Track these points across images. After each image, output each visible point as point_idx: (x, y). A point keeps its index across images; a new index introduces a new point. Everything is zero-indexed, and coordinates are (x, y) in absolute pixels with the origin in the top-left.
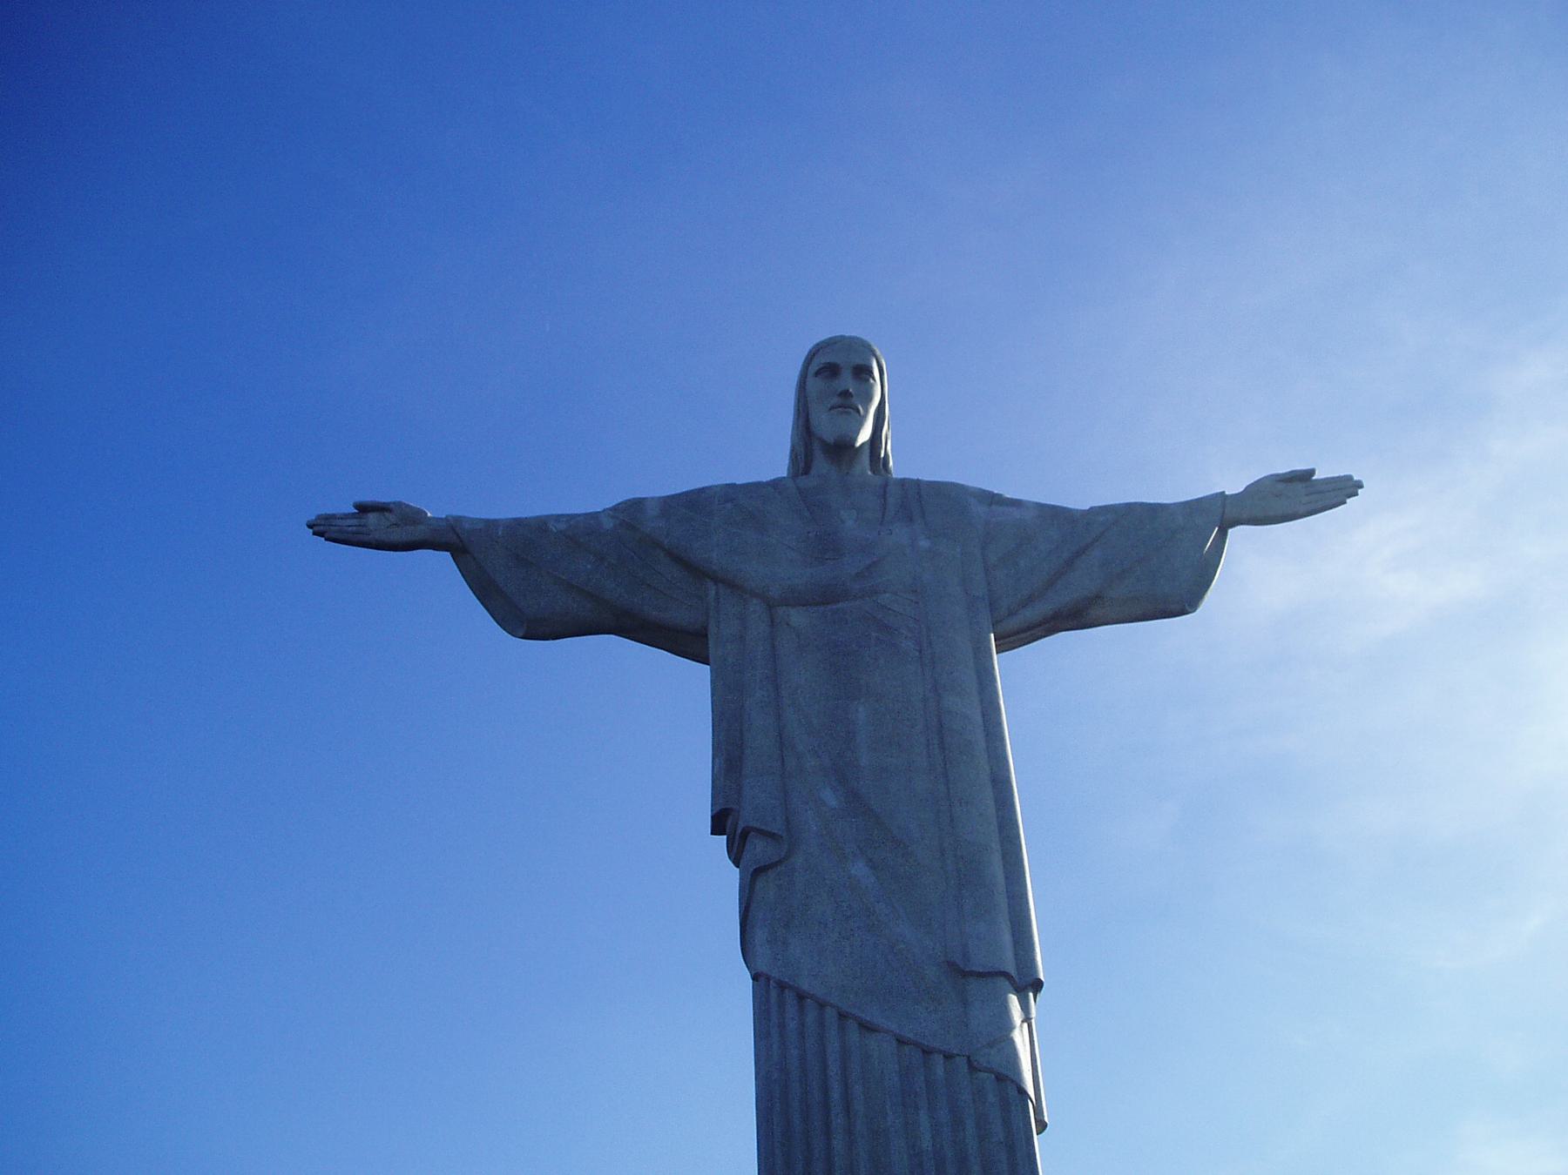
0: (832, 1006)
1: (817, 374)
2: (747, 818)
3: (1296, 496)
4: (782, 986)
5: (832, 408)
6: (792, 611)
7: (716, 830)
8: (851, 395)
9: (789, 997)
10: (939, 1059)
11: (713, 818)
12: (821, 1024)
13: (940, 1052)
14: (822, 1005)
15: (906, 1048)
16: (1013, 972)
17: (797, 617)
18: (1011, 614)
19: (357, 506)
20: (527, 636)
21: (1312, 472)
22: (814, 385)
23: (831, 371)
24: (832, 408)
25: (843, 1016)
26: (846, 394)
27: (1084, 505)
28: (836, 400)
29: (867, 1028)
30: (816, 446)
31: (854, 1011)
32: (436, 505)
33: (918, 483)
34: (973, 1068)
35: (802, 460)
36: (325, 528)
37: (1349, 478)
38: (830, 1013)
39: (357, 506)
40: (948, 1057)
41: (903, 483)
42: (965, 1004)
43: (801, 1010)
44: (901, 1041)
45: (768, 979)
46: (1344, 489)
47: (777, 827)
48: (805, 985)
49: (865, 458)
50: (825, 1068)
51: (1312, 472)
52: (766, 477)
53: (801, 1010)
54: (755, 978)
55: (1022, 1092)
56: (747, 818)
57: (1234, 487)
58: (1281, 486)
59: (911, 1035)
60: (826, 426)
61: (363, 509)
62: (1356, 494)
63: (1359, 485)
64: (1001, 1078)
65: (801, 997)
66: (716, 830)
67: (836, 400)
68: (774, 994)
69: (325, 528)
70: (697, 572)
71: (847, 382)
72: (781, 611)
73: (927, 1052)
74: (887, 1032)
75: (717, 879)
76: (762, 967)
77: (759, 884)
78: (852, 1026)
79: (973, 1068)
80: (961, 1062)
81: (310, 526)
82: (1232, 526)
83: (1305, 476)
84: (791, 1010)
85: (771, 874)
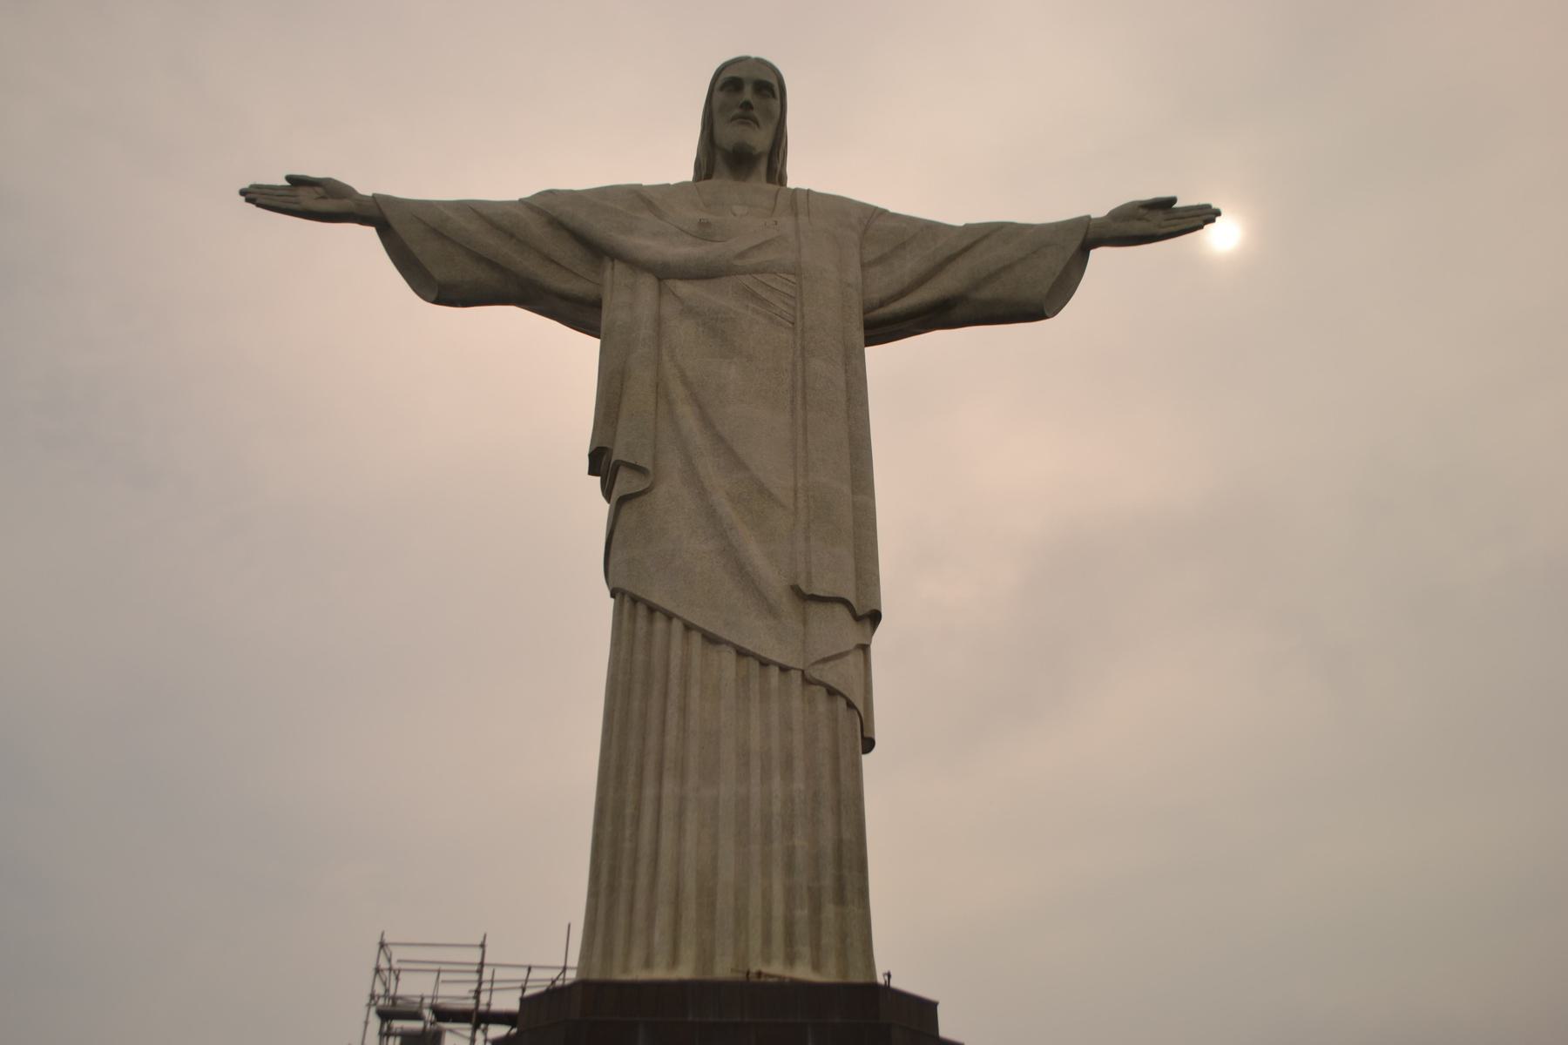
0: (678, 618)
1: (722, 88)
2: (619, 454)
3: (1159, 220)
4: (635, 600)
5: (733, 119)
6: (679, 284)
7: (592, 472)
8: (751, 108)
9: (642, 610)
10: (774, 671)
11: (590, 455)
12: (669, 633)
13: (775, 663)
14: (670, 617)
15: (744, 661)
16: (851, 598)
17: (683, 288)
18: (882, 304)
19: (289, 178)
20: (438, 301)
21: (1174, 200)
22: (719, 97)
24: (733, 119)
25: (688, 627)
26: (747, 106)
27: (959, 221)
28: (737, 111)
29: (711, 639)
30: (719, 157)
31: (701, 624)
32: (365, 185)
33: (809, 191)
34: (807, 681)
35: (705, 168)
36: (257, 196)
37: (1209, 206)
38: (677, 626)
39: (289, 178)
40: (784, 669)
41: (796, 190)
42: (805, 622)
43: (651, 620)
44: (741, 653)
45: (623, 593)
46: (1205, 215)
47: (644, 462)
48: (656, 599)
49: (762, 167)
50: (667, 673)
51: (1174, 200)
52: (673, 179)
53: (651, 620)
54: (613, 595)
55: (850, 705)
56: (619, 454)
57: (1099, 210)
58: (1142, 211)
59: (750, 647)
60: (730, 135)
61: (296, 181)
62: (1213, 221)
63: (1218, 213)
64: (832, 692)
65: (652, 609)
66: (592, 472)
67: (737, 111)
68: (627, 605)
69: (257, 196)
70: (597, 251)
71: (748, 94)
72: (670, 283)
73: (764, 663)
74: (728, 643)
75: (591, 507)
76: (621, 583)
77: (625, 510)
78: (696, 638)
79: (807, 681)
80: (796, 677)
81: (243, 193)
82: (1095, 247)
83: (1166, 204)
84: (641, 623)
85: (636, 502)
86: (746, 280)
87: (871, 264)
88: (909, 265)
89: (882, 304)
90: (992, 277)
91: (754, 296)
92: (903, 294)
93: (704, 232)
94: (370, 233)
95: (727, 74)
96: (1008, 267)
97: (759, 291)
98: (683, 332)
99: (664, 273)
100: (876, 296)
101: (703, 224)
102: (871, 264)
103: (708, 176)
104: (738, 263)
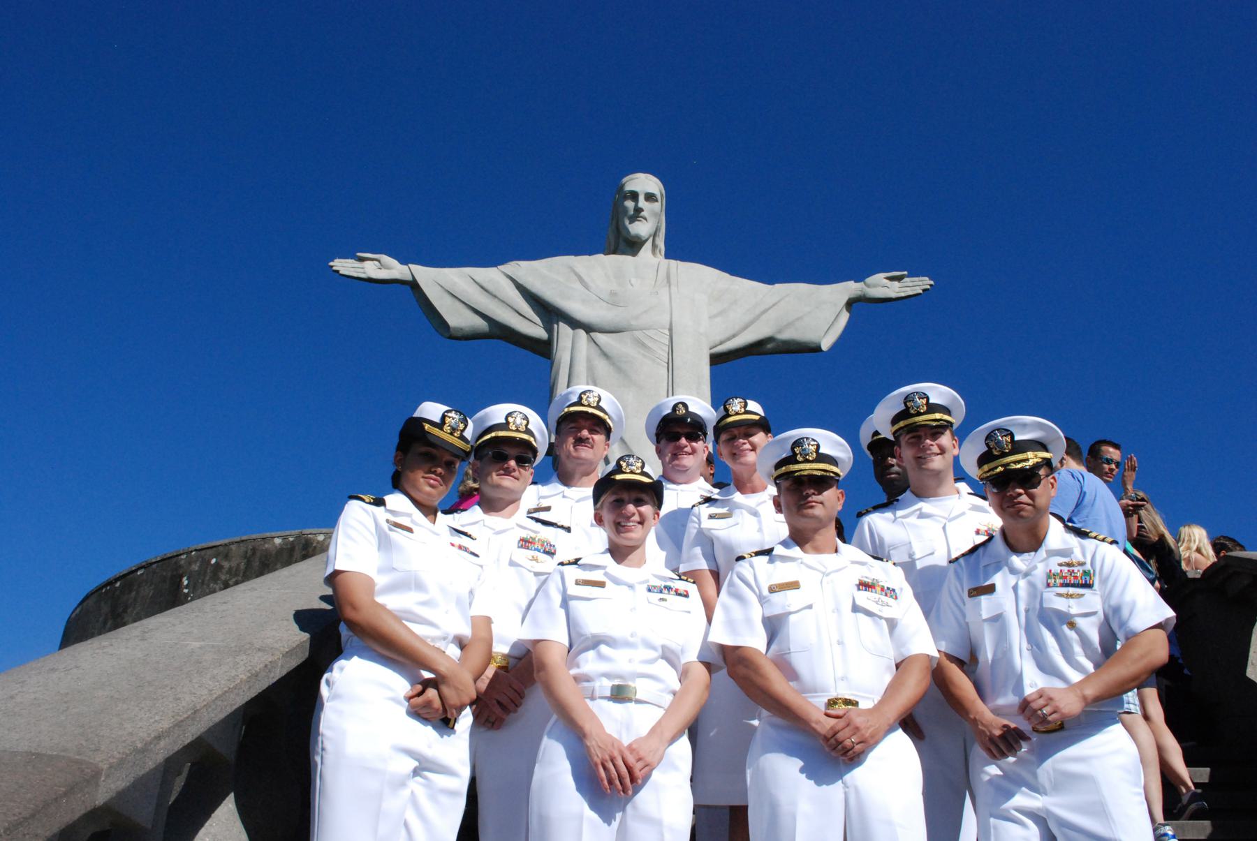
18: (721, 343)
23: (634, 196)
86: (637, 333)
87: (715, 316)
88: (737, 317)
89: (721, 343)
90: (789, 325)
91: (643, 345)
92: (734, 336)
93: (614, 300)
94: (407, 288)
95: (628, 188)
96: (798, 319)
97: (647, 342)
98: (601, 366)
99: (589, 329)
100: (718, 338)
101: (613, 294)
102: (715, 316)
103: (614, 253)
104: (634, 323)
